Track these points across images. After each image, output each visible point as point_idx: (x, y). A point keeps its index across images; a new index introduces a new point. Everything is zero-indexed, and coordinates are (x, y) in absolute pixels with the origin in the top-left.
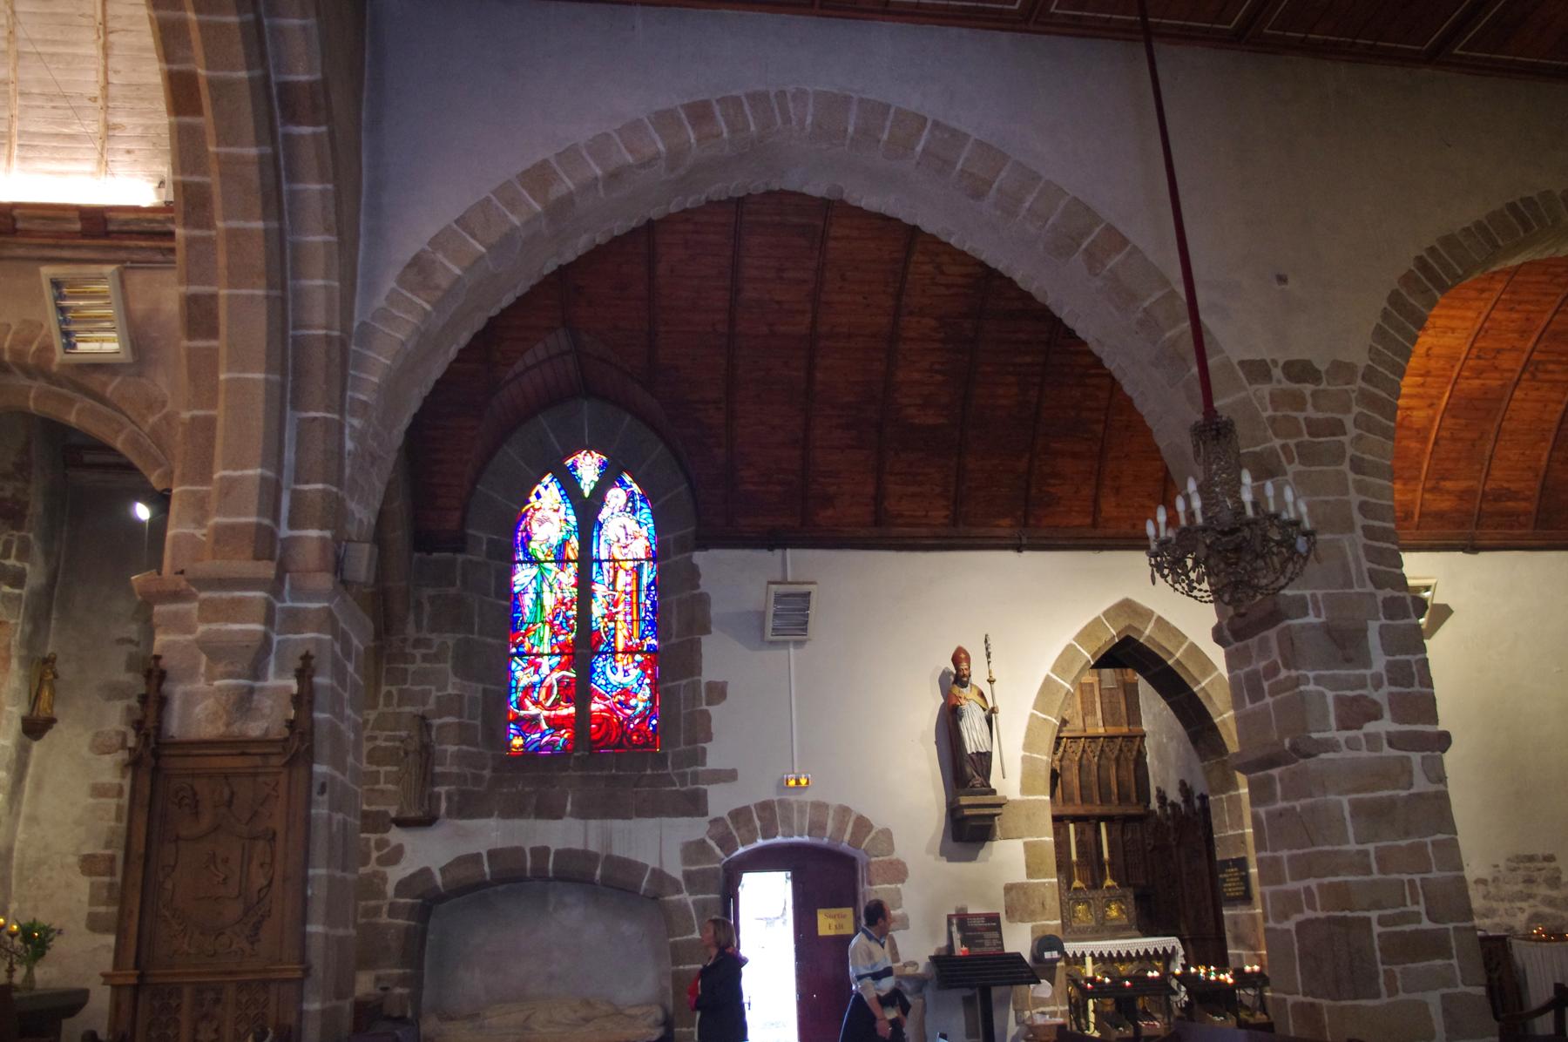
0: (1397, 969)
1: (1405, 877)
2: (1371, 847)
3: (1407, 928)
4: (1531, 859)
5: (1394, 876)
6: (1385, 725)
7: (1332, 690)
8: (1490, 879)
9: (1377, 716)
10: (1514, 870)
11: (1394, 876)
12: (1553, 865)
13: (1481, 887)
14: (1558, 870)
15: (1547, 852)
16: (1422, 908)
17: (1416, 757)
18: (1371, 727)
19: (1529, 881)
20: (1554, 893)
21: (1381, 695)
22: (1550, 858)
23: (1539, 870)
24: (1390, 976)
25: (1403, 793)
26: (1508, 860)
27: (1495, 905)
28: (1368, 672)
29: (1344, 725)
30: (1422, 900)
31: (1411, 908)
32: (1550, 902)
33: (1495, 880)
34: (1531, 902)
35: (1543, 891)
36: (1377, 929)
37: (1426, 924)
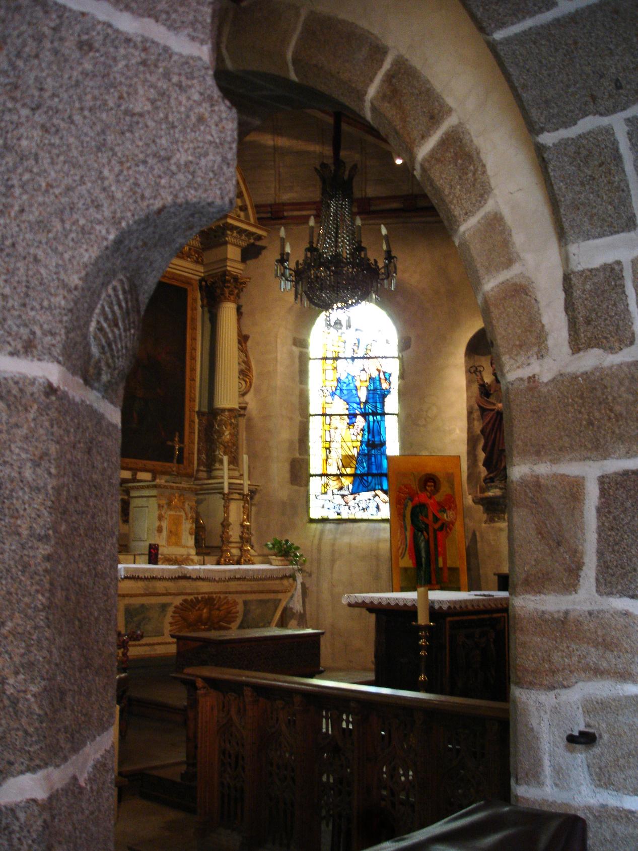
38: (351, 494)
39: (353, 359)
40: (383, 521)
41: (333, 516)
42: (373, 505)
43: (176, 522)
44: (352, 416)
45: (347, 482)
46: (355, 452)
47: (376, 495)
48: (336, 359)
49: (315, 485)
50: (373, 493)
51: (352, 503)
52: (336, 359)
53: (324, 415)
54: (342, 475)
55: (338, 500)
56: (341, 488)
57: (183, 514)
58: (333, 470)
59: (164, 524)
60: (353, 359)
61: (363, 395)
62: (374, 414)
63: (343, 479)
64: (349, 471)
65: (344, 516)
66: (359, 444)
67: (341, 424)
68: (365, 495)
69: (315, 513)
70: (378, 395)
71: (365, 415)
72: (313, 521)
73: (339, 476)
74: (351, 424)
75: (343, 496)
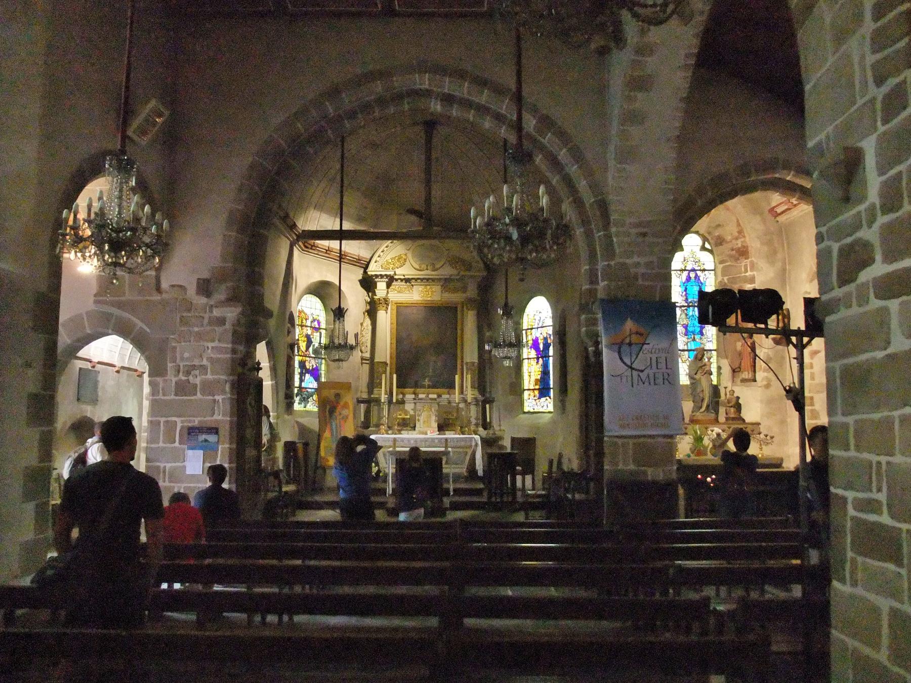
0: (860, 559)
1: (874, 458)
2: (850, 420)
3: (872, 518)
5: (866, 456)
6: (878, 269)
7: (836, 241)
9: (868, 262)
11: (866, 456)
16: (882, 497)
17: (894, 305)
18: (866, 275)
21: (870, 234)
24: (853, 561)
25: (880, 354)
28: (862, 207)
29: (843, 282)
30: (885, 489)
31: (875, 495)
36: (851, 512)
37: (885, 519)
38: (538, 399)
39: (538, 328)
40: (550, 412)
41: (532, 410)
42: (545, 405)
43: (430, 416)
44: (538, 359)
45: (537, 392)
46: (539, 377)
47: (547, 399)
48: (531, 329)
49: (526, 393)
50: (545, 398)
51: (538, 404)
52: (531, 329)
53: (528, 359)
54: (535, 389)
55: (534, 402)
56: (535, 396)
57: (431, 413)
58: (532, 387)
59: (417, 418)
60: (538, 328)
61: (541, 346)
62: (545, 357)
63: (535, 391)
64: (537, 387)
65: (535, 411)
66: (540, 373)
67: (534, 362)
68: (543, 399)
69: (526, 410)
70: (547, 346)
71: (542, 357)
72: (525, 413)
73: (534, 390)
74: (537, 362)
75: (535, 400)
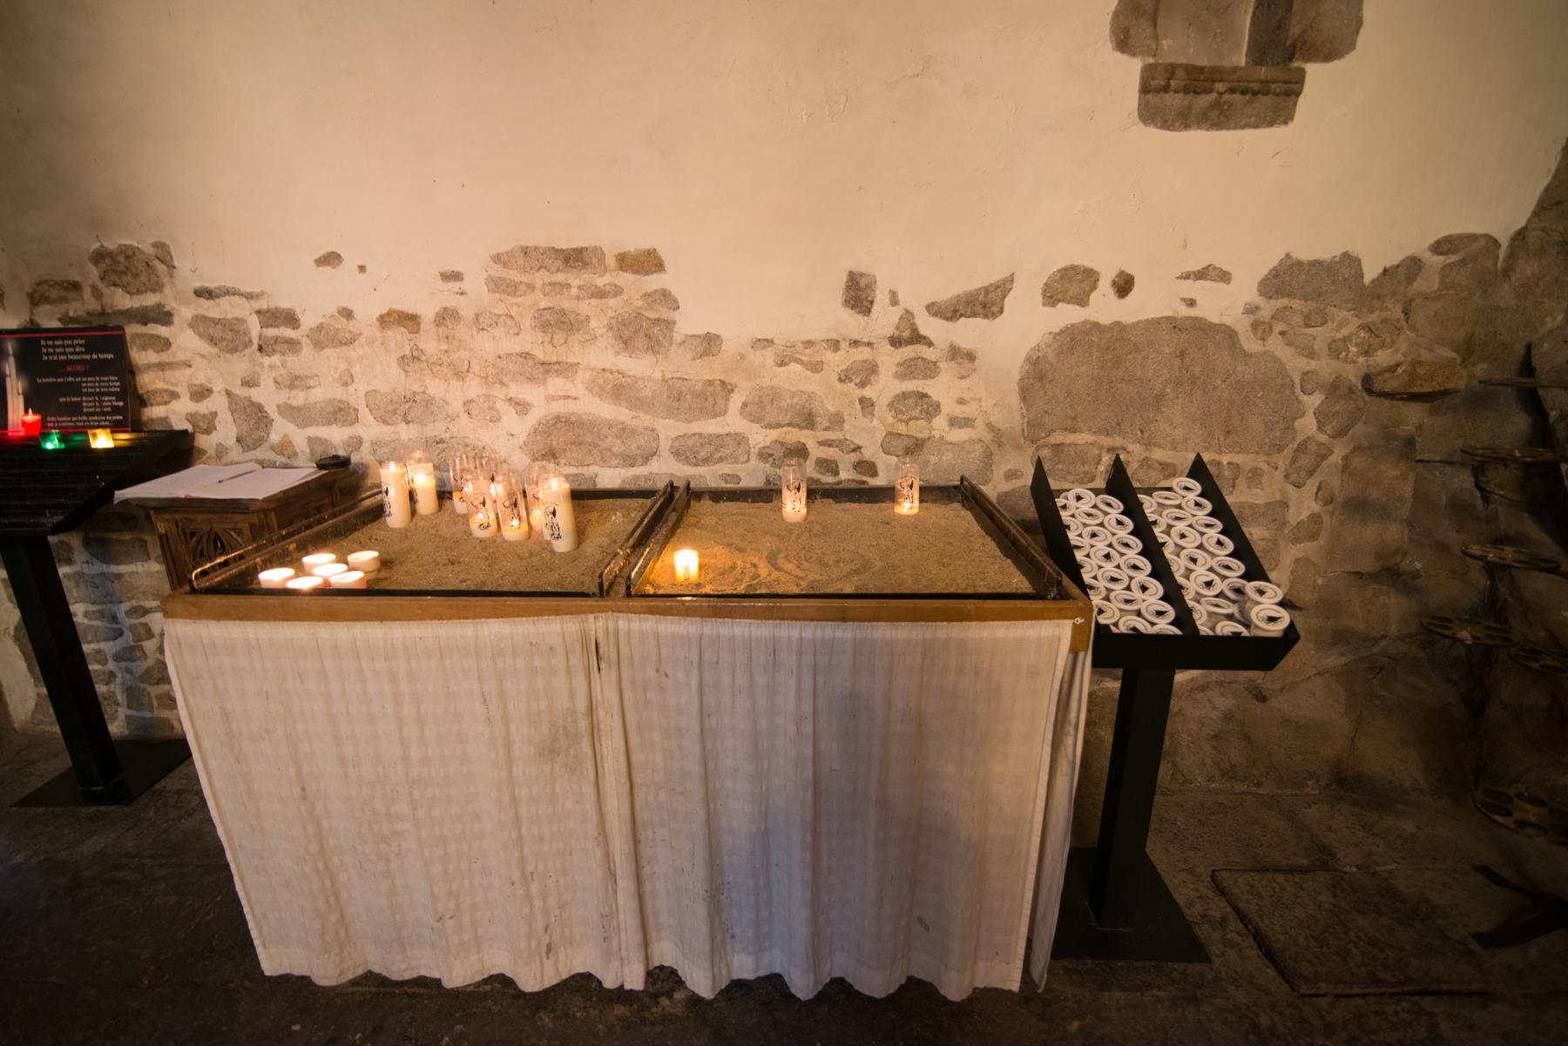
4: (575, 258)
8: (428, 312)
10: (511, 289)
12: (653, 282)
13: (398, 338)
14: (666, 298)
15: (634, 243)
19: (560, 323)
20: (639, 366)
22: (648, 262)
23: (600, 294)
26: (497, 259)
27: (435, 388)
32: (620, 390)
33: (446, 317)
34: (556, 384)
35: (601, 355)
